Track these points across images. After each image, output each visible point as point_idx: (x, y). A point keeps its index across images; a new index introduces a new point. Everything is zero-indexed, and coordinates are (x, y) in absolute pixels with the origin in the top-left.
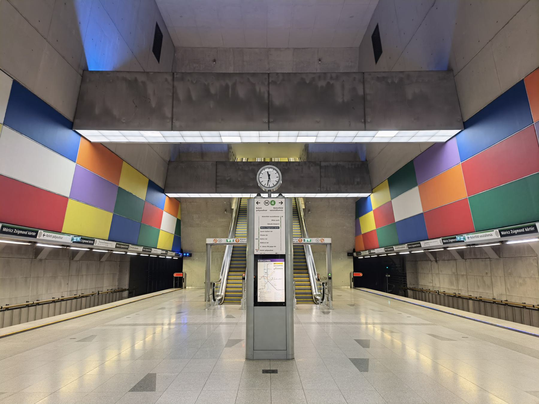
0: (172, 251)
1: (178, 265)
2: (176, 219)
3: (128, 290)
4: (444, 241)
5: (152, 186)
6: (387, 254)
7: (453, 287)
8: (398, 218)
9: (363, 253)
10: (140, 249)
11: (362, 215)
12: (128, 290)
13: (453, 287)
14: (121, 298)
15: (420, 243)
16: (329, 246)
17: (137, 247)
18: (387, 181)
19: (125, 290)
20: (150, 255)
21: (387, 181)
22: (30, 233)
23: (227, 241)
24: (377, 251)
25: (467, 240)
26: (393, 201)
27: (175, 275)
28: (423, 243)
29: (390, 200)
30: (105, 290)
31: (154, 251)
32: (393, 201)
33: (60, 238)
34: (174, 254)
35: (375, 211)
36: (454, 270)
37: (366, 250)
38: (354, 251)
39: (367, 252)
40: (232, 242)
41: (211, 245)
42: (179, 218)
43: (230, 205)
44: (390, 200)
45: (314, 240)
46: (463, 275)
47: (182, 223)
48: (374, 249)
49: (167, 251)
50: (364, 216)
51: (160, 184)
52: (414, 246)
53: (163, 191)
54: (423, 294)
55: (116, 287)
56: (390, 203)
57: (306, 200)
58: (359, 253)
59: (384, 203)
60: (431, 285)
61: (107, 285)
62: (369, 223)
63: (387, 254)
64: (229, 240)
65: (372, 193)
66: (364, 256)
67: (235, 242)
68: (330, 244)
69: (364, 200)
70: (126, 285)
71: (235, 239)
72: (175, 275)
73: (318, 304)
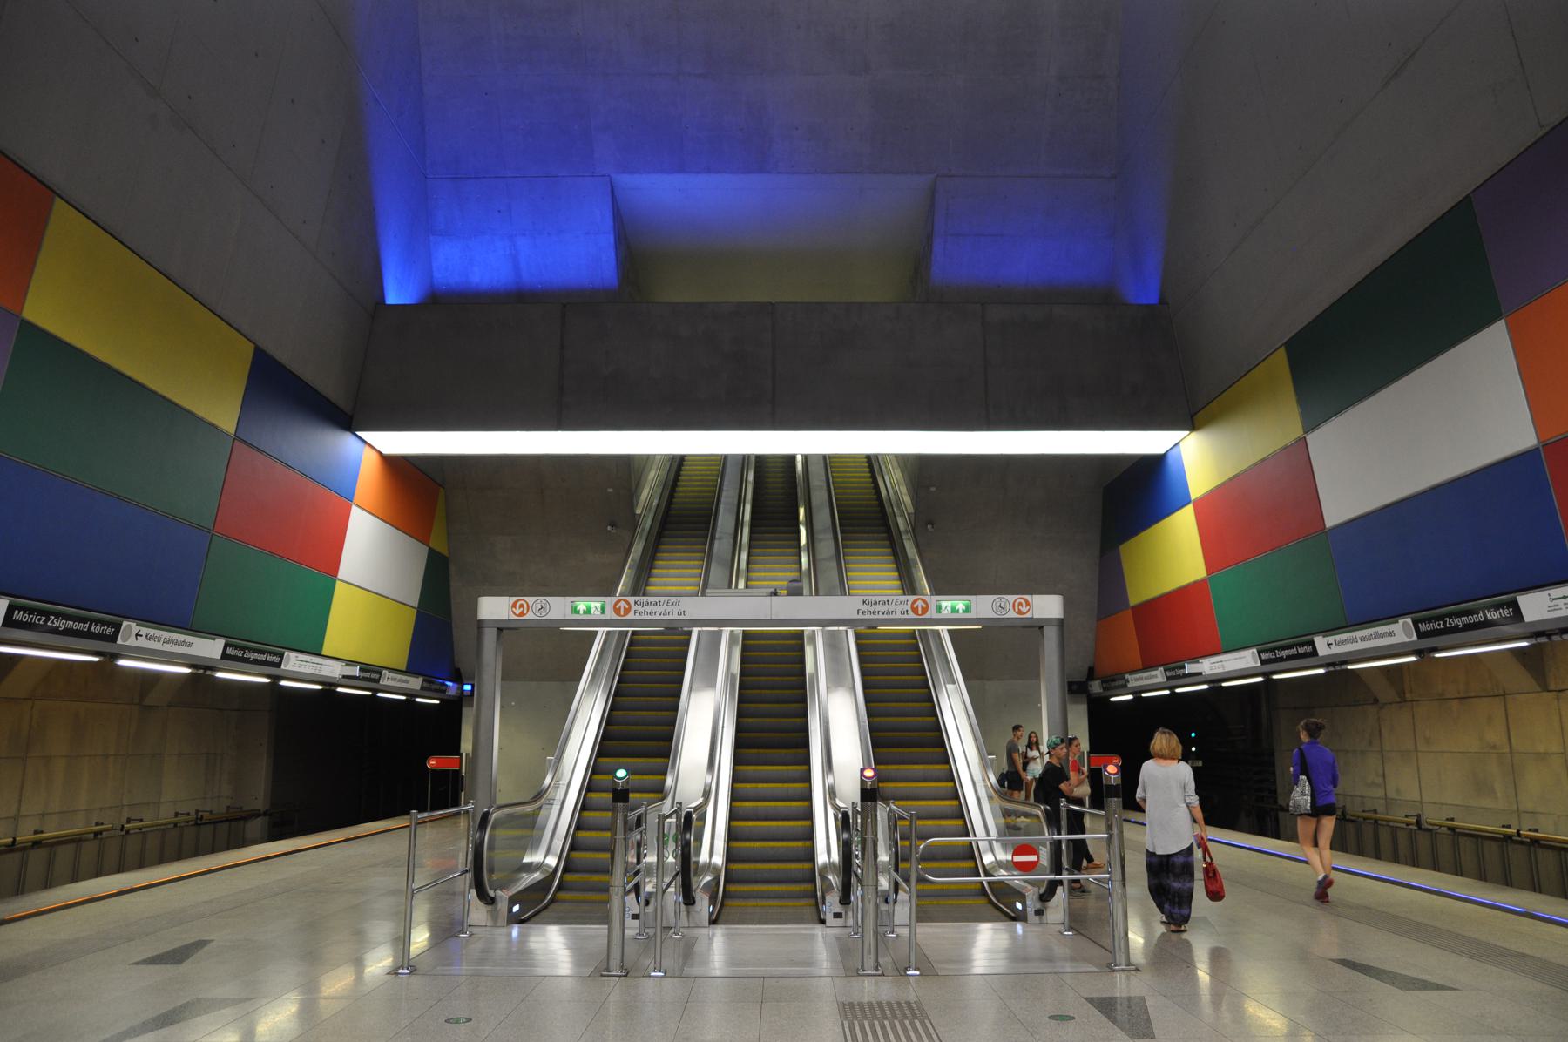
0: (411, 671)
1: (444, 726)
2: (423, 551)
3: (265, 814)
4: (1423, 627)
5: (278, 388)
6: (1266, 675)
7: (1486, 802)
8: (1336, 512)
9: (1135, 681)
10: (211, 649)
11: (1149, 526)
12: (265, 814)
13: (1486, 802)
14: (241, 842)
15: (1312, 643)
16: (1051, 635)
17: (189, 639)
18: (1281, 357)
19: (255, 814)
20: (375, 691)
21: (1282, 350)
22: (95, 629)
23: (575, 611)
24: (1209, 666)
25: (1529, 616)
26: (1309, 438)
27: (432, 763)
28: (1324, 646)
29: (1299, 432)
30: (166, 814)
31: (294, 662)
32: (1313, 439)
33: (184, 643)
34: (415, 683)
35: (1202, 507)
36: (1495, 735)
37: (1148, 666)
38: (1091, 673)
39: (1159, 676)
40: (596, 614)
41: (502, 628)
42: (442, 549)
43: (631, 496)
44: (1299, 432)
45: (984, 607)
46: (1542, 757)
47: (453, 569)
48: (1194, 659)
49: (378, 670)
50: (1143, 535)
51: (329, 384)
52: (1460, 622)
53: (349, 422)
54: (1351, 827)
55: (219, 807)
56: (1302, 443)
57: (921, 468)
58: (1114, 681)
59: (1245, 466)
60: (1380, 793)
61: (175, 795)
62: (1177, 552)
63: (1266, 675)
64: (582, 606)
65: (1192, 425)
66: (1137, 692)
67: (610, 615)
68: (1061, 623)
69: (1152, 468)
70: (258, 794)
71: (610, 601)
72: (432, 763)
73: (1019, 917)
